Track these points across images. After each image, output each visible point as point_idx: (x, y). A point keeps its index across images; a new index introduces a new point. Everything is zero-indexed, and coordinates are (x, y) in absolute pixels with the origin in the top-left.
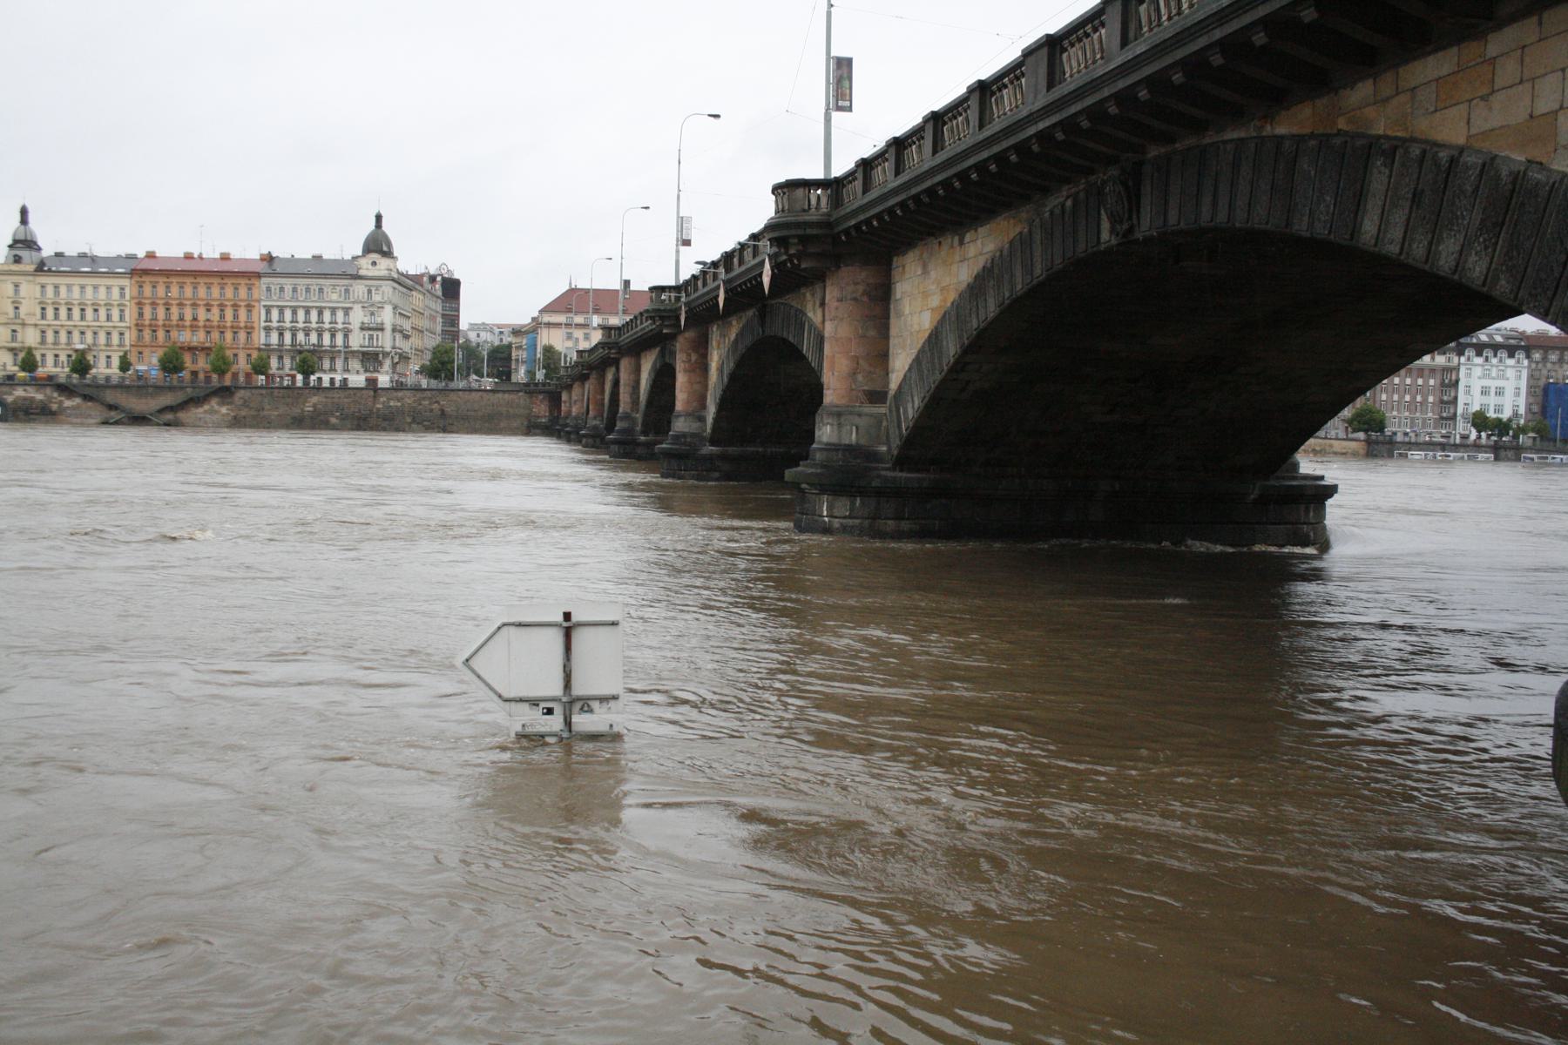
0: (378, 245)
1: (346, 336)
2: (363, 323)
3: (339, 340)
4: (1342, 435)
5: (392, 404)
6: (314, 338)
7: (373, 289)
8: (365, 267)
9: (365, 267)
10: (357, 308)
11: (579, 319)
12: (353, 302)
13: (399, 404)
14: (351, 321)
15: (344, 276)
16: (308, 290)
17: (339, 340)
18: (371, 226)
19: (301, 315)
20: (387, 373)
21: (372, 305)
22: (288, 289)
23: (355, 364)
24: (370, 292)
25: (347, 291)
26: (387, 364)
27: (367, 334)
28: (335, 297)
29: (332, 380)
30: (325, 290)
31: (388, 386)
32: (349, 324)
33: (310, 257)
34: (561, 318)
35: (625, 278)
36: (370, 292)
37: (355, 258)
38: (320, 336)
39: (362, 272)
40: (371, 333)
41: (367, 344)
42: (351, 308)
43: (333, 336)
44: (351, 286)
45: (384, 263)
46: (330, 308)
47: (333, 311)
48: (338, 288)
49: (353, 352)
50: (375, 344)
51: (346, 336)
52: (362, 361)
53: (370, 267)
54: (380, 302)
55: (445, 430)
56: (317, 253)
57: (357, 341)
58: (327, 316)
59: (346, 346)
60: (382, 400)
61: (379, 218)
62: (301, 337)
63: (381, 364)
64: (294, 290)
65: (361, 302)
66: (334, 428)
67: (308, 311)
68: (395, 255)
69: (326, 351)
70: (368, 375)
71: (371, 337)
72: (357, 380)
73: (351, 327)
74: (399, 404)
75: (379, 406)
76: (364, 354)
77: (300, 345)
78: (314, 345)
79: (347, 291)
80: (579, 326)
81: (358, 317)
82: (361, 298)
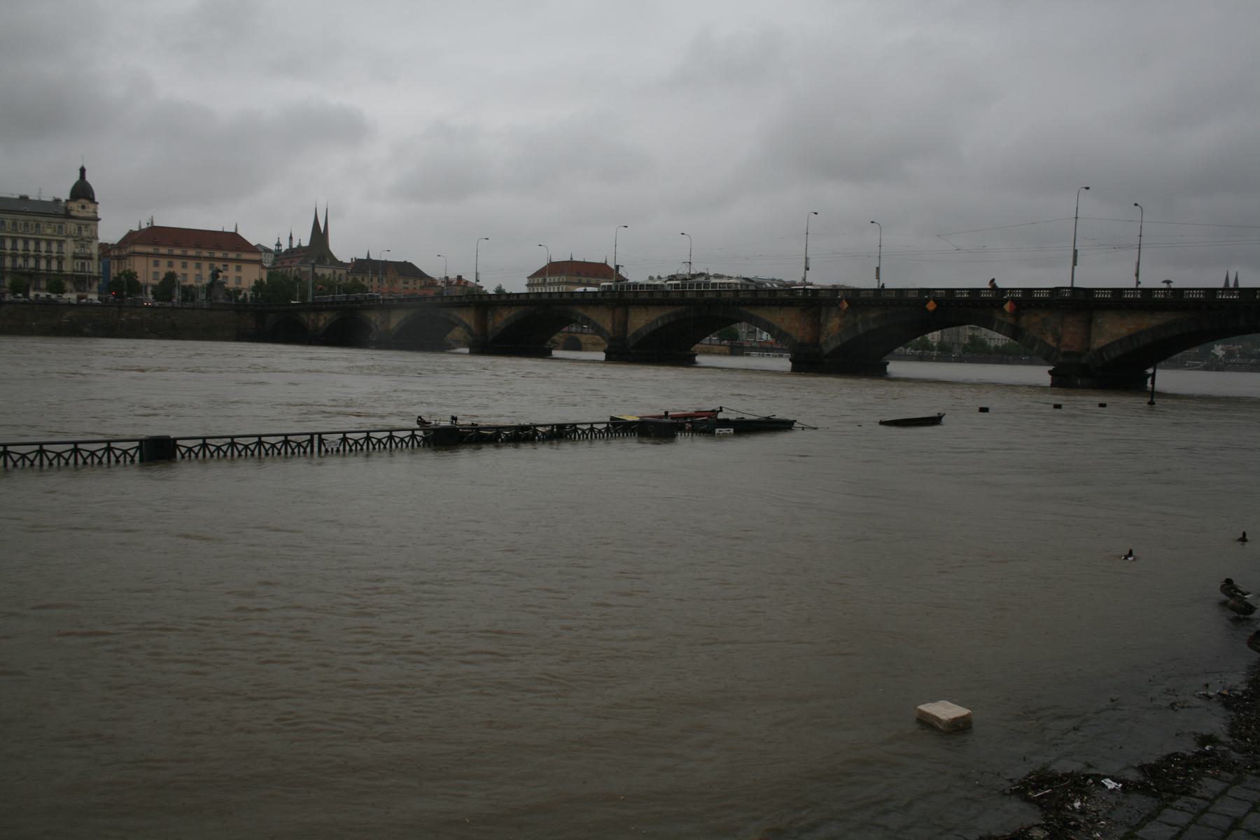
0: (82, 191)
1: (60, 263)
2: (74, 253)
3: (54, 266)
4: (718, 343)
5: (133, 317)
6: (32, 263)
7: (83, 227)
8: (76, 209)
9: (75, 208)
10: (69, 240)
11: (206, 254)
12: (67, 236)
13: (139, 318)
14: (64, 250)
15: (56, 215)
16: (26, 225)
17: (54, 266)
18: (76, 177)
19: (20, 244)
20: (94, 292)
21: (82, 239)
22: (8, 222)
23: (69, 286)
24: (80, 229)
25: (60, 227)
26: (95, 288)
27: (80, 262)
28: (49, 231)
29: (37, 296)
30: (42, 225)
31: (75, 303)
32: (63, 253)
33: (16, 196)
34: (150, 250)
35: (617, 264)
36: (80, 229)
37: (57, 201)
38: (37, 262)
39: (74, 213)
40: (83, 261)
41: (80, 269)
42: (64, 241)
43: (49, 262)
44: (64, 223)
45: (91, 206)
46: (45, 240)
47: (49, 242)
48: (53, 225)
49: (66, 276)
50: (86, 270)
51: (60, 263)
52: (75, 283)
53: (80, 209)
54: (89, 237)
55: (174, 337)
56: (23, 193)
57: (68, 267)
58: (43, 246)
59: (60, 270)
60: (126, 314)
61: (83, 171)
62: (20, 261)
63: (90, 285)
64: (14, 224)
65: (73, 237)
66: (87, 335)
67: (26, 241)
68: (96, 200)
69: (54, 274)
70: (80, 294)
71: (83, 265)
72: (71, 297)
73: (65, 256)
74: (139, 318)
75: (123, 319)
76: (78, 277)
77: (20, 268)
78: (32, 269)
79: (60, 227)
80: (206, 258)
81: (70, 248)
82: (72, 233)
